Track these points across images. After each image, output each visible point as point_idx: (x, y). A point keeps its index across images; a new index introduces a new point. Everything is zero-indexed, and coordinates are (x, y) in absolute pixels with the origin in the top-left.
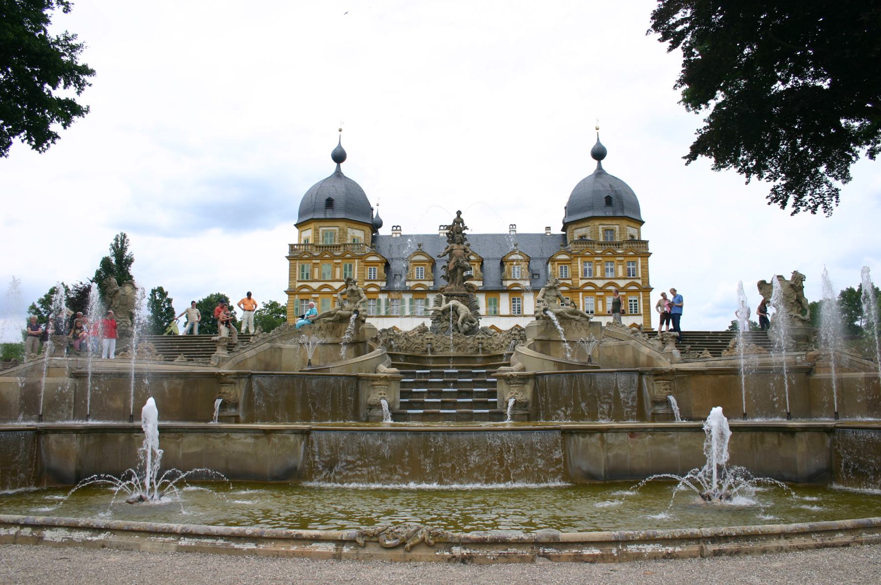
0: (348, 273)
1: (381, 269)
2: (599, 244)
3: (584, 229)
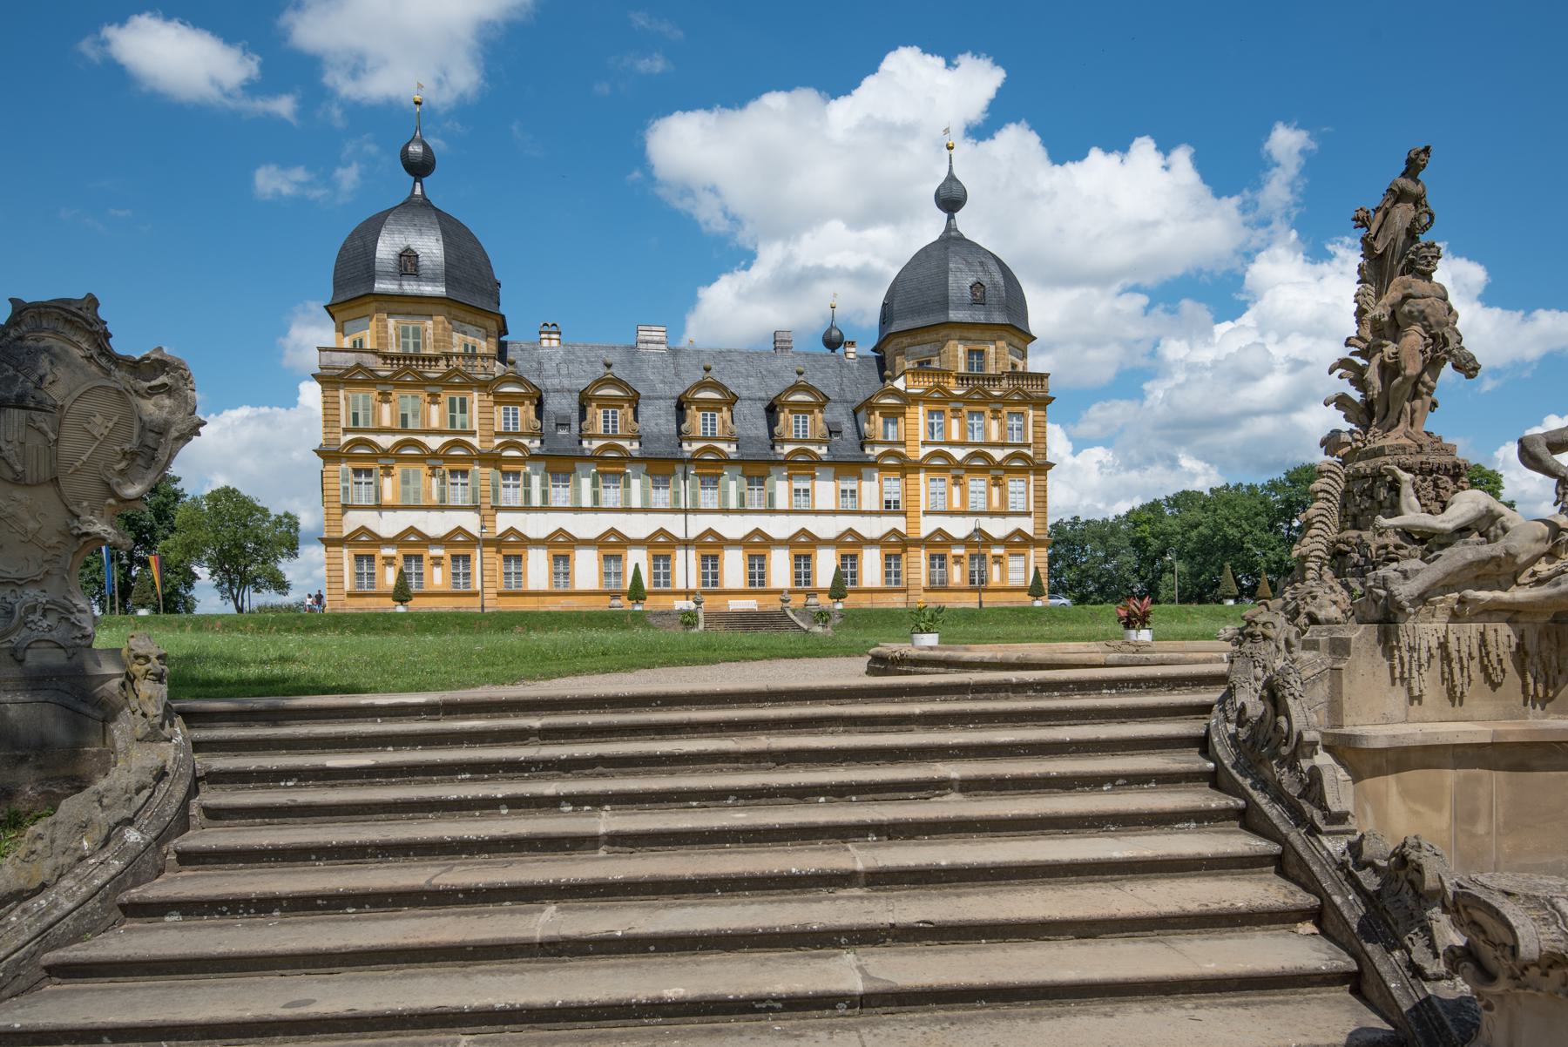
0: (458, 415)
1: (526, 412)
2: (957, 378)
3: (928, 347)
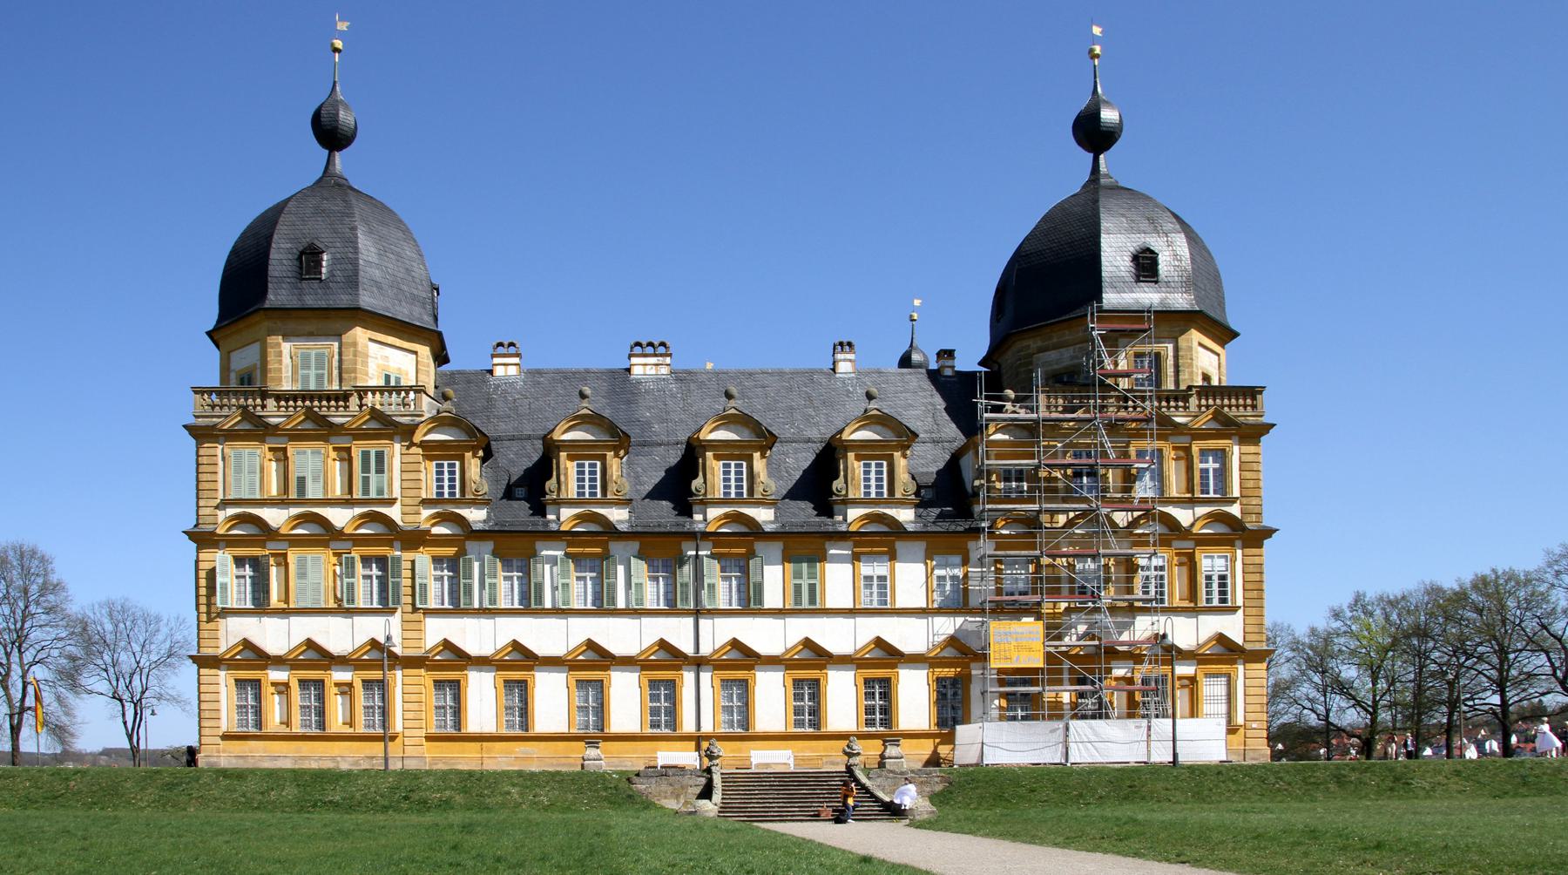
0: (373, 476)
